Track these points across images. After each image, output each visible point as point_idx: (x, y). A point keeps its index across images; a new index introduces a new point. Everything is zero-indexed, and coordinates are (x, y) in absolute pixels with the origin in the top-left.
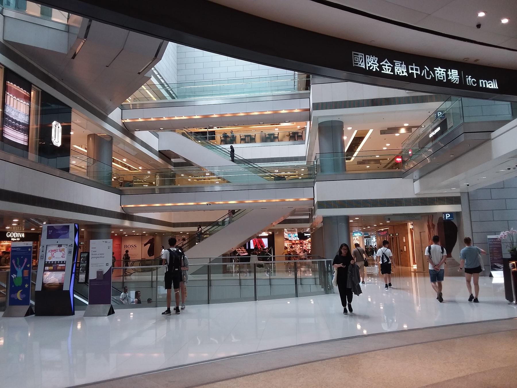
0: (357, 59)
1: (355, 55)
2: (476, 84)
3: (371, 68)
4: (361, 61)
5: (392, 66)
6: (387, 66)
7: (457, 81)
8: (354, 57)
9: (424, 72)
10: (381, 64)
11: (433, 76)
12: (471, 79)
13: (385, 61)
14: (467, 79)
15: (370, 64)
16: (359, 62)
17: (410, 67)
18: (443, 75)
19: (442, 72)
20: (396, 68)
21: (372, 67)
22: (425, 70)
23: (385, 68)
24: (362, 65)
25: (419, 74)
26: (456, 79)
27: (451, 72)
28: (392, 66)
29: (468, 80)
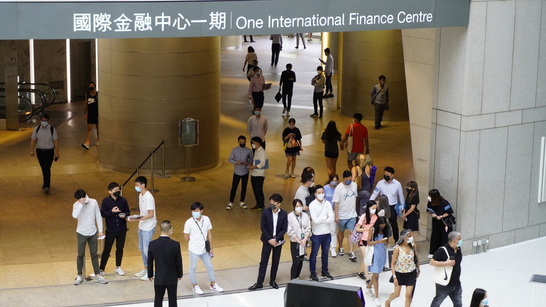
1: (77, 18)
4: (85, 23)
6: (123, 22)
8: (76, 20)
9: (177, 21)
10: (115, 21)
17: (157, 18)
20: (137, 23)
24: (87, 27)
25: (169, 25)
28: (131, 21)
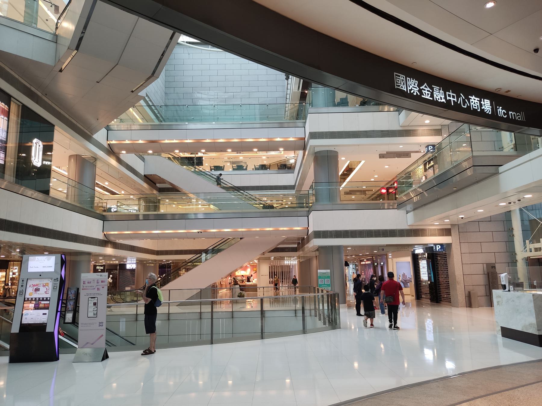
0: (398, 81)
1: (396, 77)
2: (506, 116)
3: (412, 92)
4: (402, 84)
5: (431, 91)
6: (426, 90)
7: (489, 112)
8: (396, 78)
9: (460, 100)
10: (421, 88)
11: (469, 105)
12: (501, 110)
13: (424, 86)
14: (498, 109)
15: (411, 87)
16: (401, 84)
17: (447, 93)
18: (477, 104)
19: (476, 101)
20: (435, 94)
21: (413, 91)
22: (461, 97)
23: (425, 93)
24: (404, 87)
25: (456, 101)
26: (488, 110)
27: (484, 102)
28: (431, 91)
29: (499, 111)
